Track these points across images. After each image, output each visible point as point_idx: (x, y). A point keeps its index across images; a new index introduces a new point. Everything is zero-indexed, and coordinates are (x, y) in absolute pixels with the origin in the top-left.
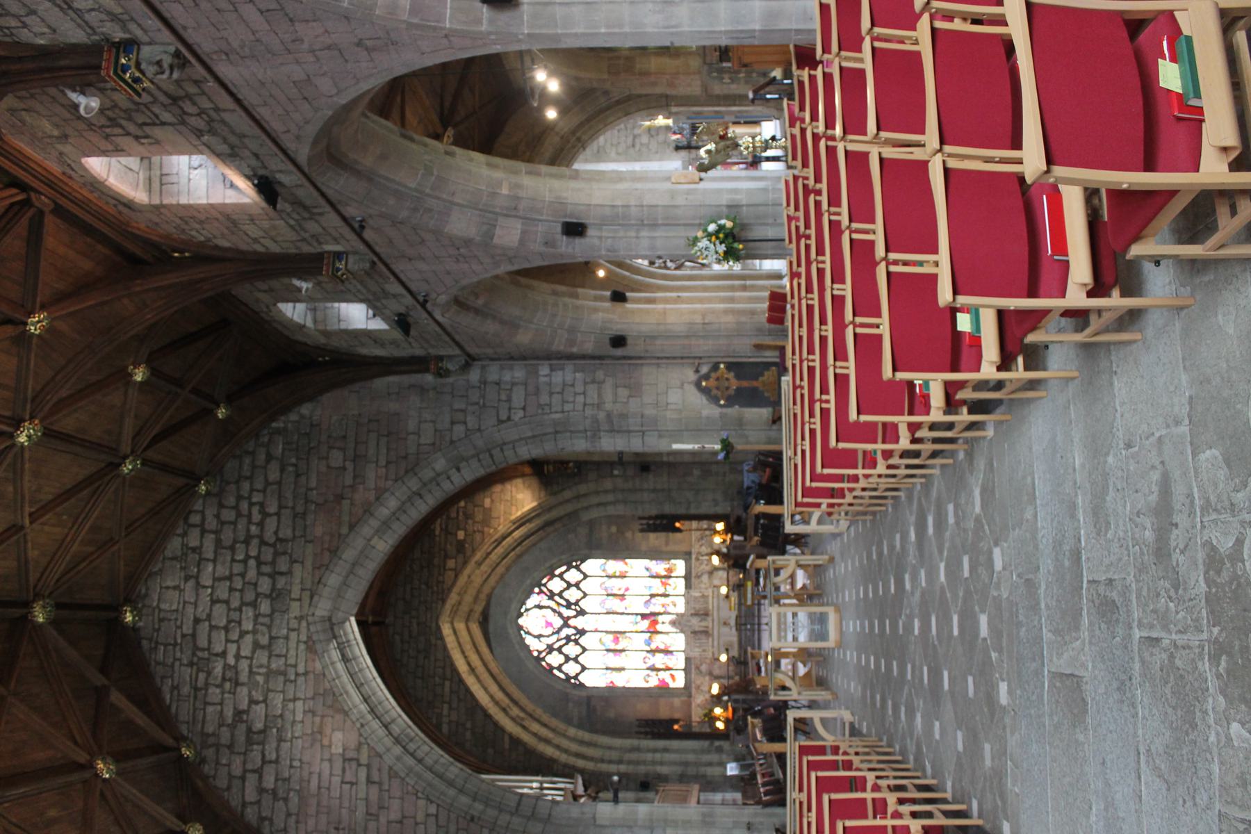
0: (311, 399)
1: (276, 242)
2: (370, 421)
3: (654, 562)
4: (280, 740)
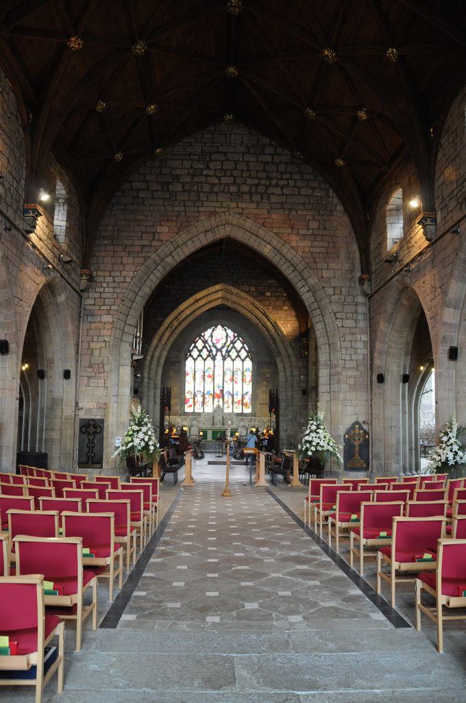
0: (346, 210)
1: (442, 184)
2: (334, 242)
4: (164, 199)
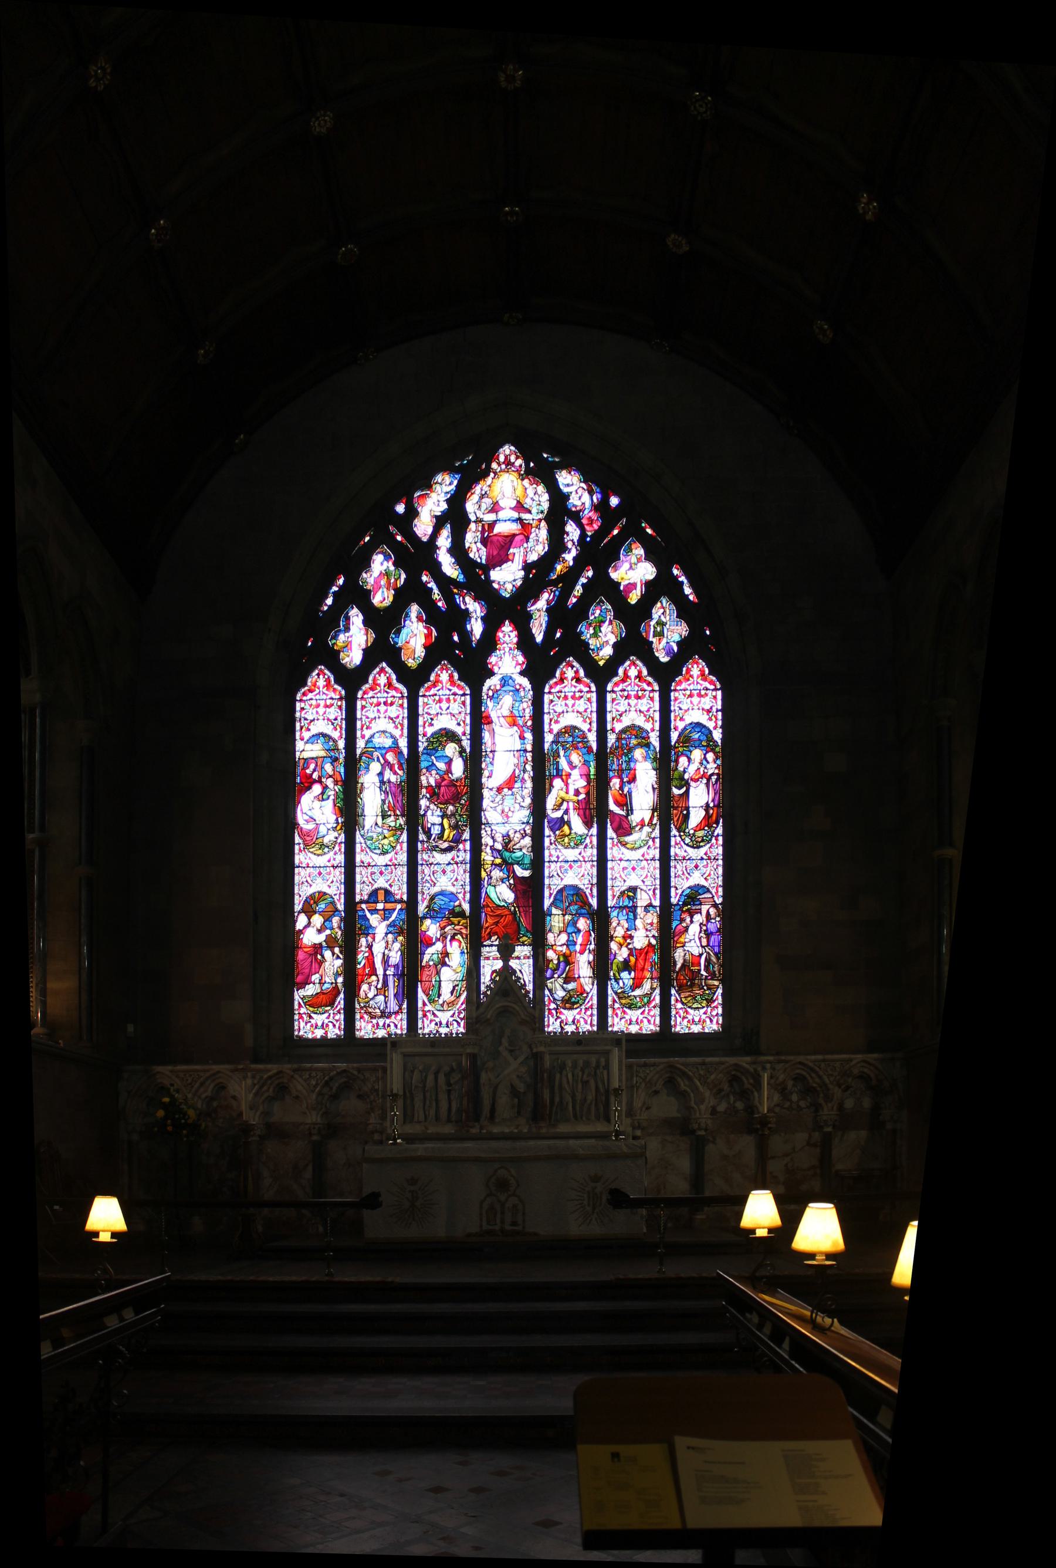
3: (714, 925)
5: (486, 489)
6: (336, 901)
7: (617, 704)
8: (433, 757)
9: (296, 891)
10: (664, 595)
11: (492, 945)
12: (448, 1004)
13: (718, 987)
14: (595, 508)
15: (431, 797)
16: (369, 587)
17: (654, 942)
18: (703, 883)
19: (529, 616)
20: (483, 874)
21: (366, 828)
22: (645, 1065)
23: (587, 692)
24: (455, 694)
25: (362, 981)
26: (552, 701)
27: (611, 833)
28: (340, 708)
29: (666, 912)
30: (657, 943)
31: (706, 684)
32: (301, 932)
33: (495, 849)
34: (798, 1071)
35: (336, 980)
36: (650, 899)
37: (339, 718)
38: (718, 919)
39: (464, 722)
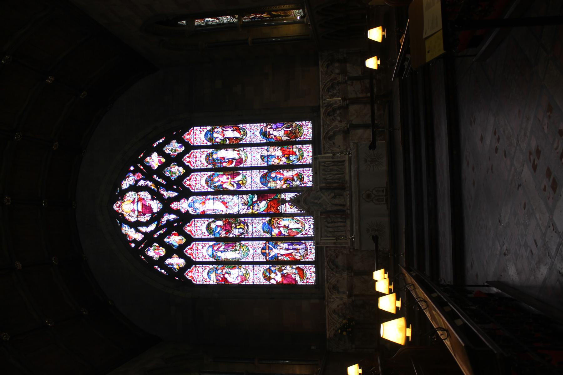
3: (273, 126)
5: (127, 214)
6: (266, 268)
7: (198, 165)
8: (216, 232)
9: (262, 284)
10: (162, 149)
11: (281, 209)
12: (302, 225)
13: (295, 123)
14: (134, 175)
15: (229, 233)
16: (159, 257)
17: (280, 148)
18: (259, 131)
19: (169, 198)
20: (256, 213)
21: (240, 257)
22: (324, 148)
23: (194, 176)
24: (194, 224)
25: (294, 258)
26: (197, 189)
27: (242, 166)
28: (199, 267)
29: (269, 144)
30: (280, 147)
31: (192, 133)
32: (277, 282)
33: (247, 208)
34: (326, 90)
35: (294, 268)
36: (265, 150)
37: (202, 267)
38: (272, 125)
39: (204, 221)
